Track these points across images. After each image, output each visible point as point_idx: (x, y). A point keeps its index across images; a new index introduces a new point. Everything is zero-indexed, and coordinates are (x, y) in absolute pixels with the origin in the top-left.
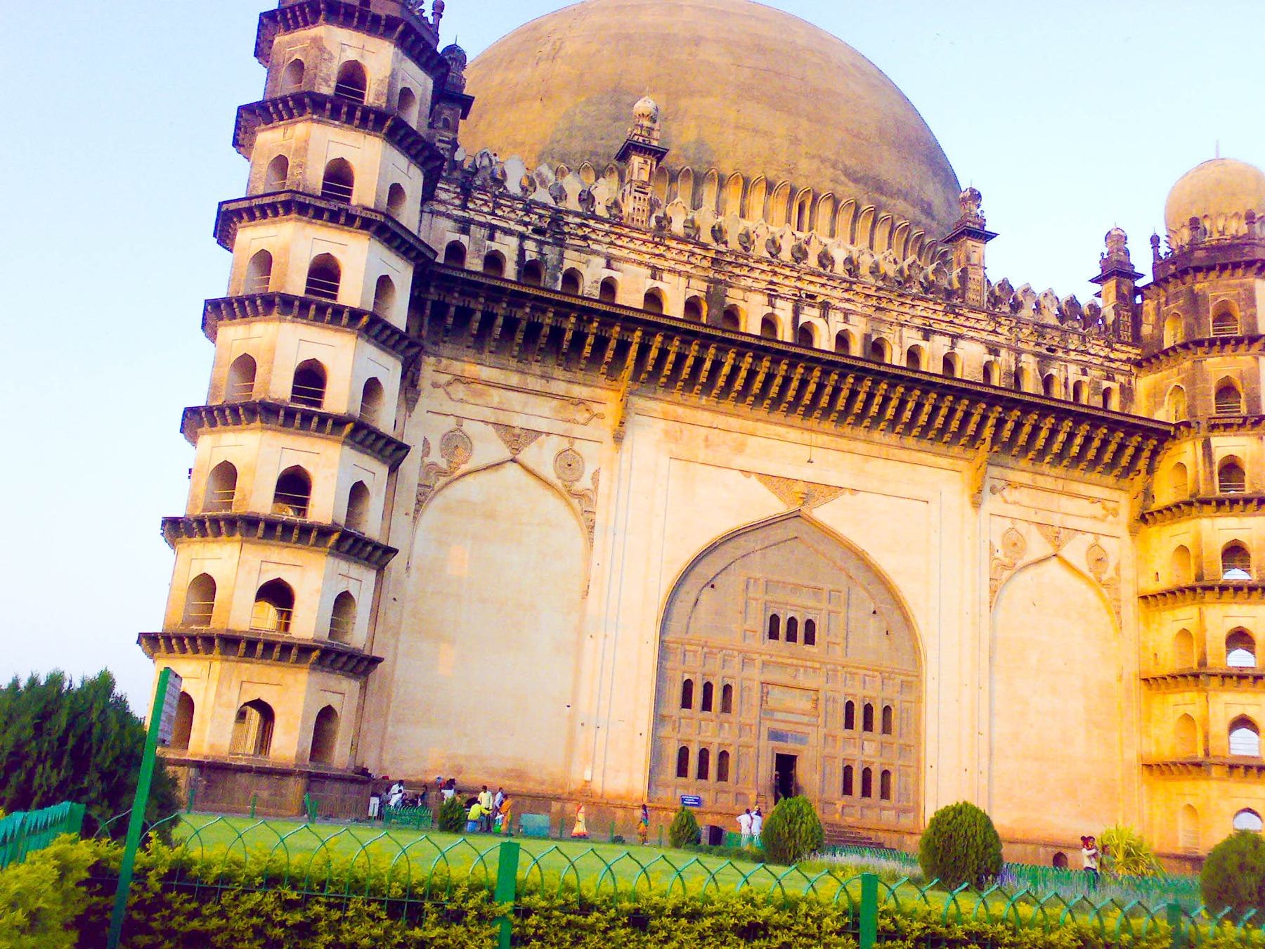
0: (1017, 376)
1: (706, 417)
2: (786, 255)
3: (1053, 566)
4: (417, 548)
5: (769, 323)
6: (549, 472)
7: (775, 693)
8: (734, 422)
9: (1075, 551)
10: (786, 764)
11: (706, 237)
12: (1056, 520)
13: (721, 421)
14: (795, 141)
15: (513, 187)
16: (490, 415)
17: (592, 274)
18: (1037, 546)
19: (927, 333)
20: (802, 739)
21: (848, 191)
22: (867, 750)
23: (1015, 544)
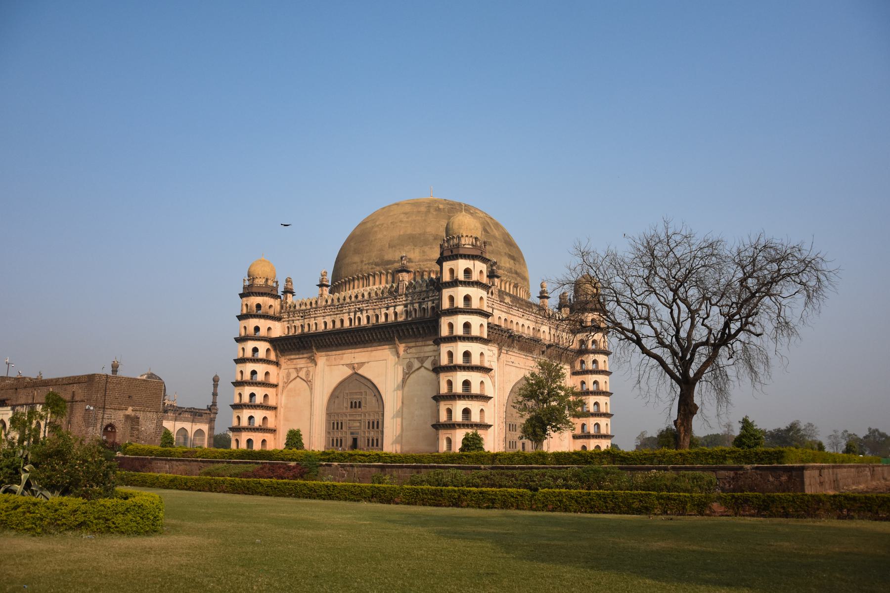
0: (415, 310)
1: (334, 353)
2: (353, 299)
3: (423, 369)
4: (283, 402)
5: (350, 320)
6: (304, 377)
7: (351, 423)
8: (340, 352)
9: (428, 364)
10: (355, 440)
11: (336, 302)
12: (422, 355)
13: (338, 352)
14: (362, 262)
15: (298, 307)
16: (293, 366)
17: (312, 322)
18: (417, 365)
19: (387, 308)
20: (358, 433)
21: (377, 269)
22: (372, 434)
23: (410, 366)
